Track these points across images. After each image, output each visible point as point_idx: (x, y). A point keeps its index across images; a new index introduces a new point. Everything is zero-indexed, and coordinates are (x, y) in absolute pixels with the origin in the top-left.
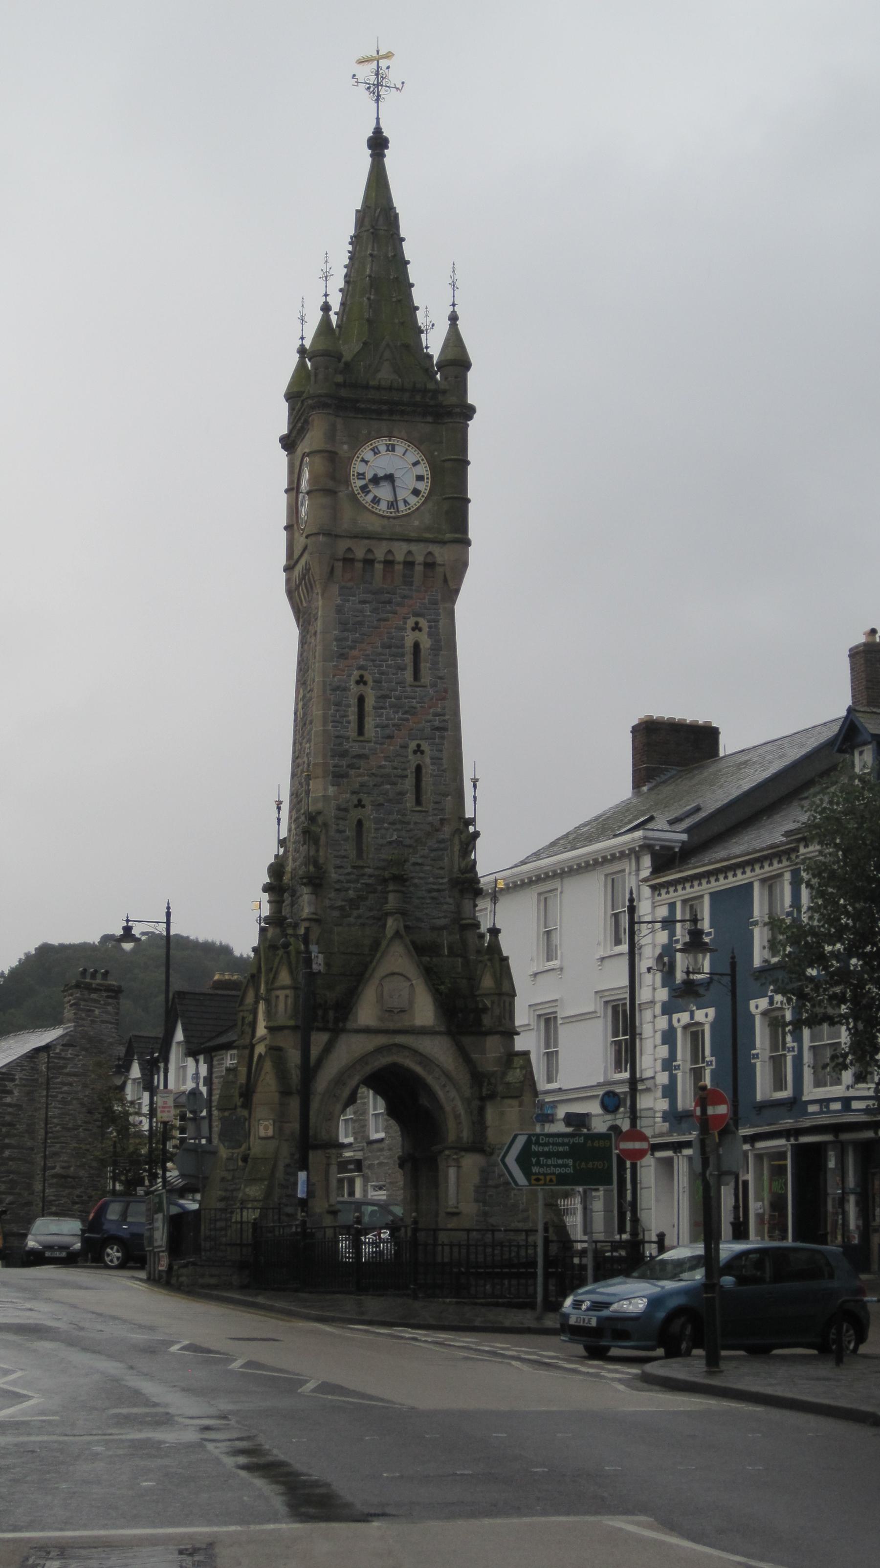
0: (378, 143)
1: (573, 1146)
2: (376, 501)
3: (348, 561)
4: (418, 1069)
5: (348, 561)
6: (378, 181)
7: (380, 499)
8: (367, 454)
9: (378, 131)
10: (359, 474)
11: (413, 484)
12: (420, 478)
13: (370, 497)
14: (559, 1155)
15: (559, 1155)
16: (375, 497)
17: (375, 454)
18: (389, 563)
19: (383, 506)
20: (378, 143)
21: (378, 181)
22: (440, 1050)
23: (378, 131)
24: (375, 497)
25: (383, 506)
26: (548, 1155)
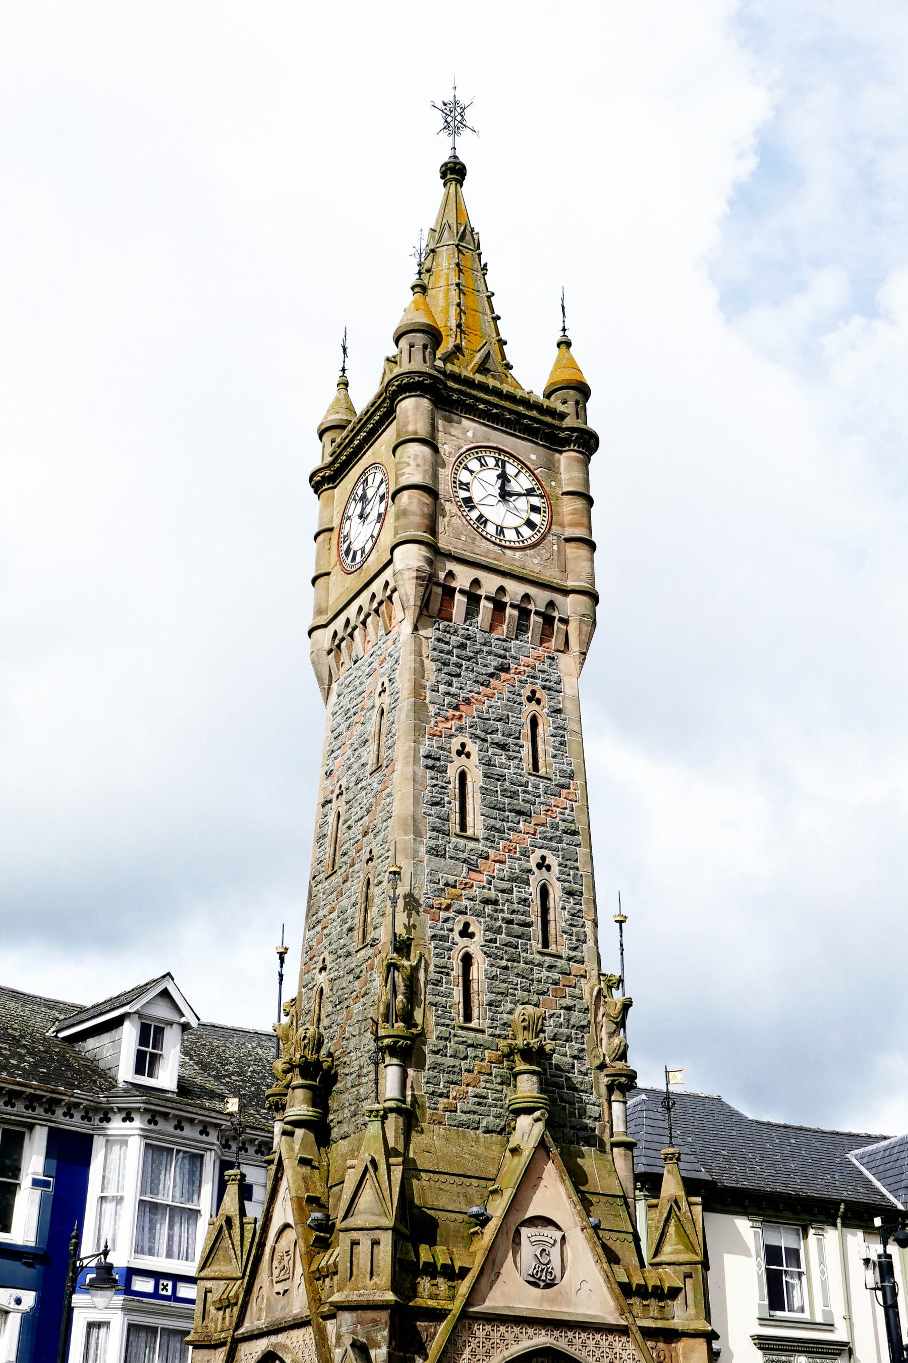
2: (482, 520)
6: (456, 207)
7: (487, 520)
10: (461, 483)
13: (474, 514)
16: (481, 516)
17: (482, 465)
19: (491, 529)
20: (454, 172)
21: (456, 207)
24: (481, 516)
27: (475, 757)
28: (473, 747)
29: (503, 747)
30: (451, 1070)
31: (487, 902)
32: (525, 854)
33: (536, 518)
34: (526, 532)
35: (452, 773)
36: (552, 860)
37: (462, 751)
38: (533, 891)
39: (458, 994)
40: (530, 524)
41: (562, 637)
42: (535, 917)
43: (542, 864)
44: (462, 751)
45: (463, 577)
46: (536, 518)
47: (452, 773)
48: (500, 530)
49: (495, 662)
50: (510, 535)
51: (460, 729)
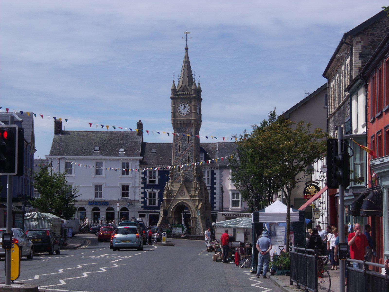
0: (187, 49)
2: (181, 113)
6: (187, 56)
9: (187, 46)
19: (183, 114)
20: (187, 49)
21: (187, 56)
23: (187, 46)
25: (183, 114)
27: (181, 143)
28: (181, 142)
29: (184, 141)
30: (177, 177)
31: (181, 159)
32: (186, 153)
33: (189, 110)
34: (187, 113)
35: (178, 146)
36: (190, 153)
37: (179, 143)
38: (187, 157)
39: (178, 169)
40: (188, 111)
41: (192, 125)
42: (187, 160)
43: (188, 154)
44: (179, 143)
46: (189, 110)
47: (178, 146)
48: (184, 114)
49: (183, 131)
50: (185, 114)
51: (179, 140)
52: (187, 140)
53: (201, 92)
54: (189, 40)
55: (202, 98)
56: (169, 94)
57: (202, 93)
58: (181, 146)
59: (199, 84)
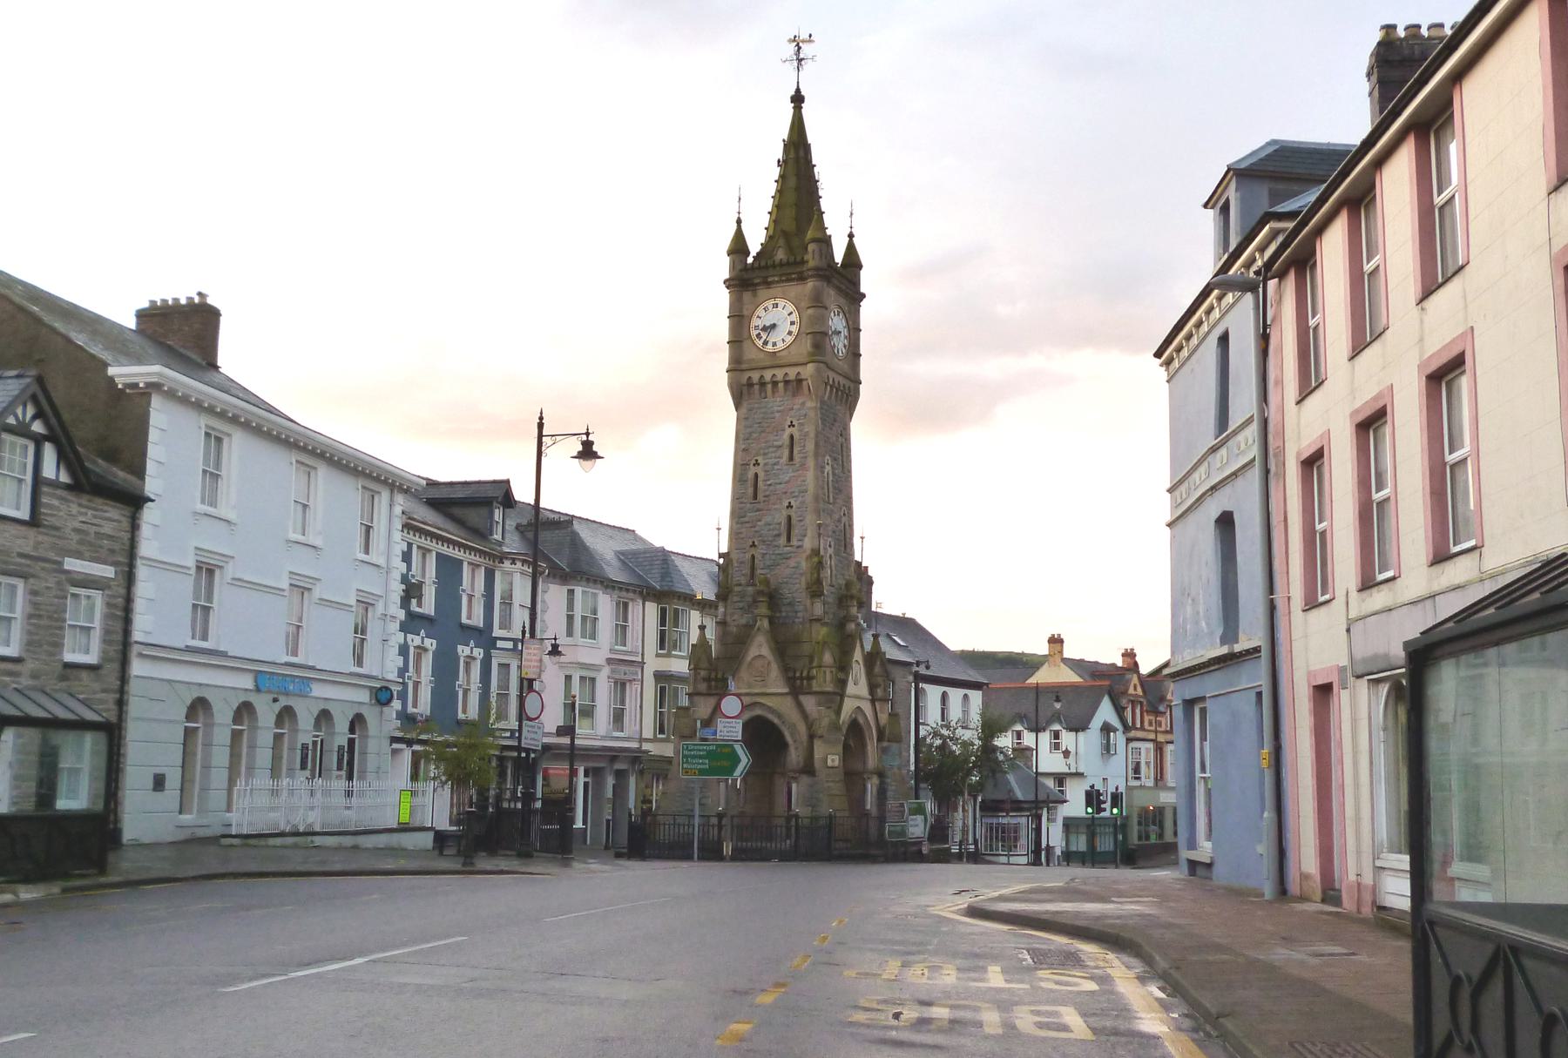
0: (798, 99)
1: (709, 752)
3: (750, 384)
4: (776, 721)
5: (750, 384)
6: (798, 126)
8: (760, 311)
9: (798, 90)
11: (788, 327)
12: (792, 323)
14: (701, 757)
15: (701, 757)
18: (775, 384)
20: (798, 99)
21: (798, 126)
22: (786, 706)
23: (798, 90)
26: (694, 757)
40: (790, 333)
45: (755, 376)
47: (751, 475)
48: (774, 344)
52: (786, 453)
53: (860, 267)
54: (807, 66)
55: (863, 289)
56: (722, 267)
57: (863, 273)
58: (761, 476)
59: (851, 236)
